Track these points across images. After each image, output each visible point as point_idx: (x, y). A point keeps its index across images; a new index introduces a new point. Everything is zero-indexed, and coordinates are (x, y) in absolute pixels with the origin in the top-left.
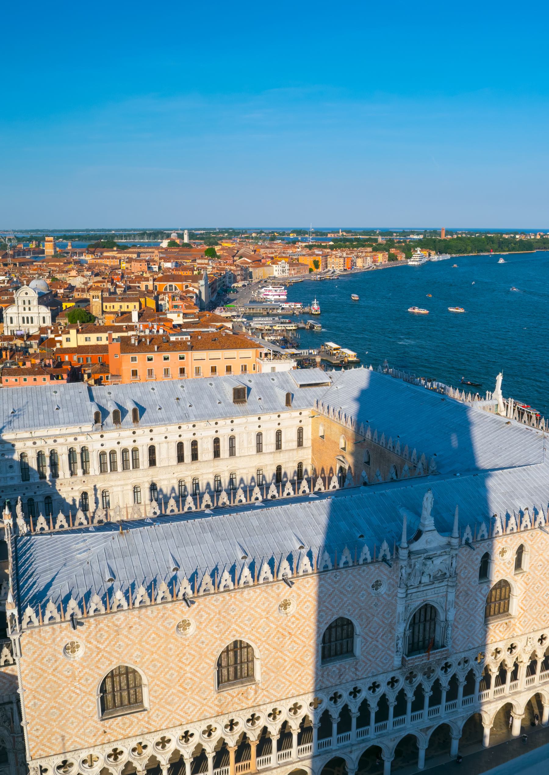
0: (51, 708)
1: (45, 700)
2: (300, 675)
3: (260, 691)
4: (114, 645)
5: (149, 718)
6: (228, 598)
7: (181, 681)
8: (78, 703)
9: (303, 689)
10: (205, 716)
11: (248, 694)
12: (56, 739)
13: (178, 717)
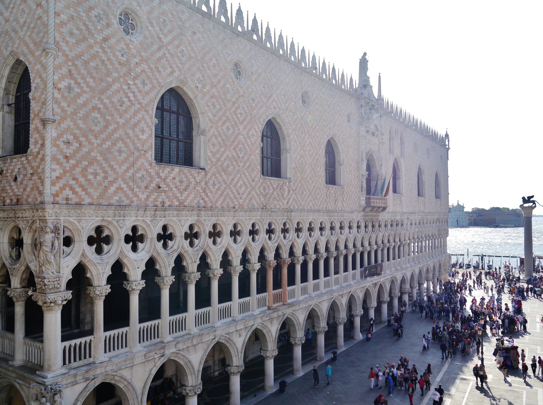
0: (95, 108)
1: (85, 89)
2: (314, 186)
3: (291, 192)
4: (178, 46)
5: (206, 183)
6: (271, 58)
7: (236, 143)
8: (131, 118)
9: (316, 204)
10: (253, 205)
11: (284, 190)
12: (96, 174)
13: (232, 196)
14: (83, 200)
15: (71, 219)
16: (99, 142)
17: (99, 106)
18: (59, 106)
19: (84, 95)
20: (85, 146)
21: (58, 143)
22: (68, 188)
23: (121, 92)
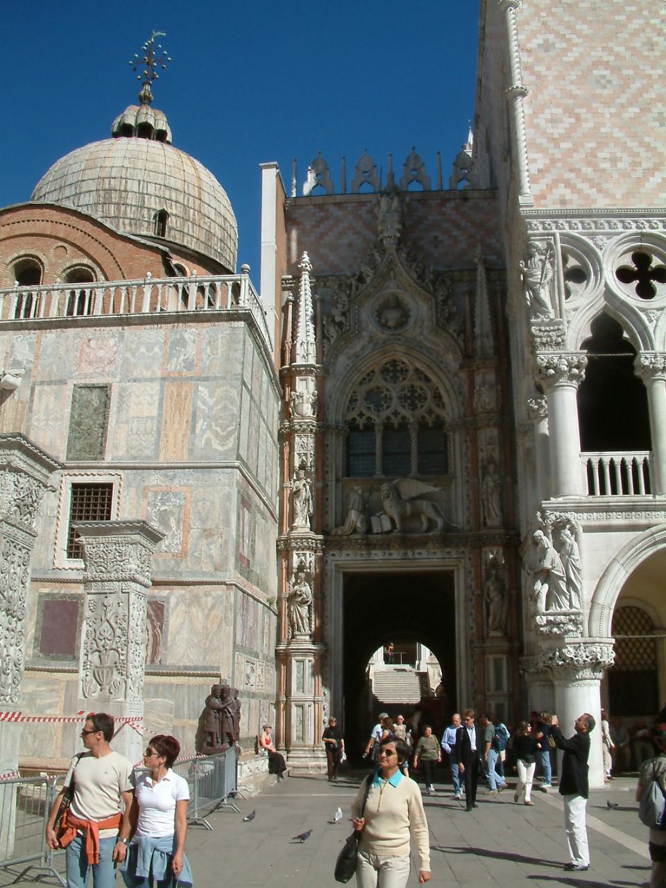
0: (596, 64)
1: (575, 40)
12: (614, 160)
14: (595, 201)
15: (574, 233)
16: (613, 110)
17: (605, 59)
18: (533, 73)
19: (574, 49)
20: (587, 120)
21: (535, 121)
22: (562, 186)
23: (648, 30)
